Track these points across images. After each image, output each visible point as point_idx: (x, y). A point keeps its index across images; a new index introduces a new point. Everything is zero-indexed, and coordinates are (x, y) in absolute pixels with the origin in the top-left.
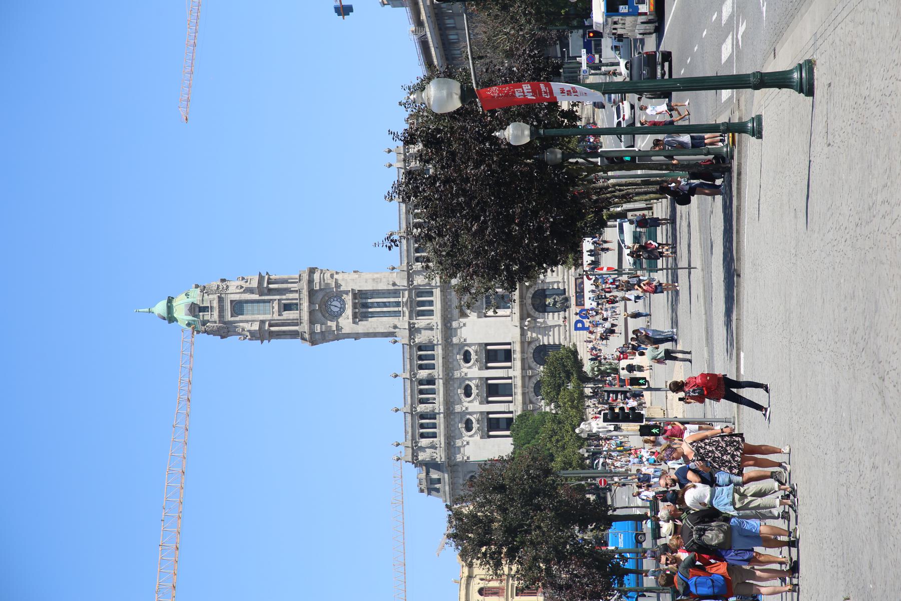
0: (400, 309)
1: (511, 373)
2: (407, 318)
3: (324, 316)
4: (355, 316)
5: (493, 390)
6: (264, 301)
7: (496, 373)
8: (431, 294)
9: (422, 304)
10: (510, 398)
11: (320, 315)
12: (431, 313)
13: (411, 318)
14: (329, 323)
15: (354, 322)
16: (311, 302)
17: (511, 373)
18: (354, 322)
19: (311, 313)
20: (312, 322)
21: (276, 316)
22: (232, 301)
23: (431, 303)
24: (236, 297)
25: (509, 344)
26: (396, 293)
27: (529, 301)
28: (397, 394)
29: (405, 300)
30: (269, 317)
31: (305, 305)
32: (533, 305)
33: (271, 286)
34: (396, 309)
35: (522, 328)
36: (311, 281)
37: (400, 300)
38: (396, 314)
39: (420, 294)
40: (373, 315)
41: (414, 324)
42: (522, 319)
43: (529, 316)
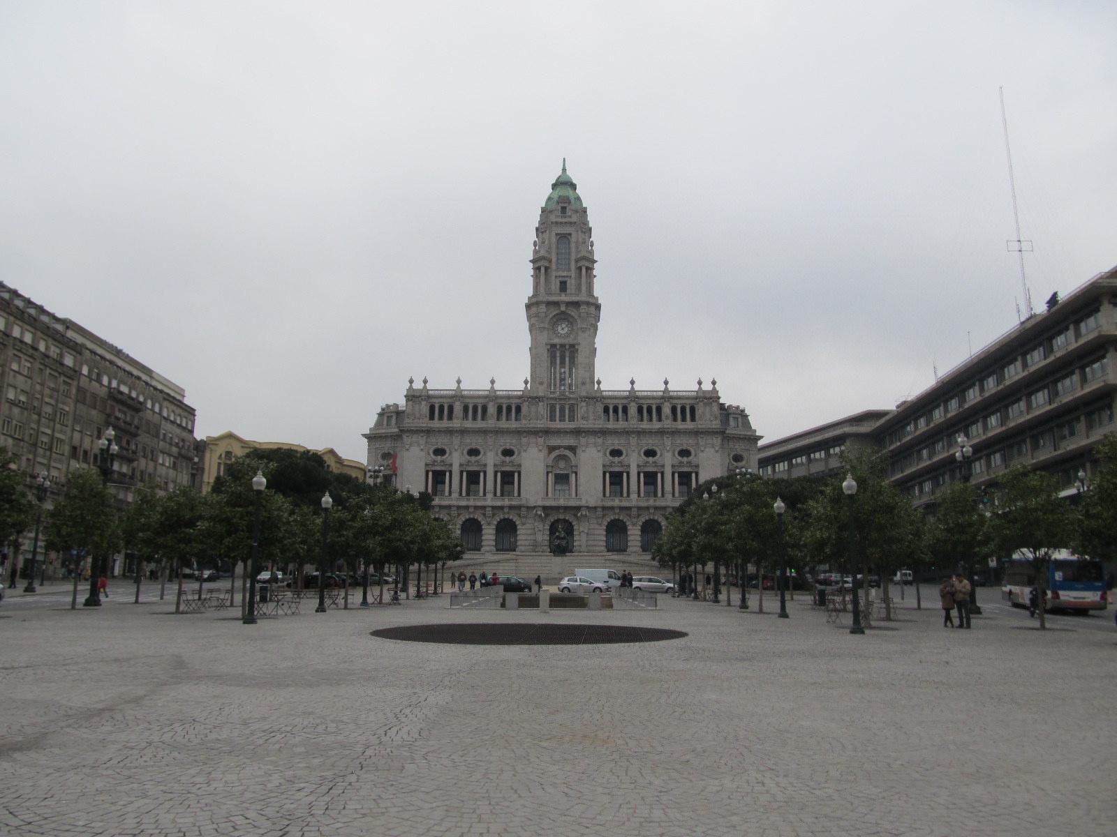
1: (490, 496)
3: (554, 316)
4: (553, 346)
5: (473, 478)
7: (490, 481)
8: (572, 419)
9: (562, 410)
10: (464, 493)
11: (555, 313)
12: (552, 419)
16: (569, 304)
17: (490, 496)
19: (557, 304)
21: (554, 274)
22: (570, 234)
23: (562, 419)
24: (573, 239)
25: (519, 495)
27: (562, 517)
28: (476, 383)
30: (554, 266)
31: (563, 298)
32: (557, 521)
33: (584, 270)
35: (535, 507)
36: (588, 304)
42: (545, 508)
43: (547, 515)
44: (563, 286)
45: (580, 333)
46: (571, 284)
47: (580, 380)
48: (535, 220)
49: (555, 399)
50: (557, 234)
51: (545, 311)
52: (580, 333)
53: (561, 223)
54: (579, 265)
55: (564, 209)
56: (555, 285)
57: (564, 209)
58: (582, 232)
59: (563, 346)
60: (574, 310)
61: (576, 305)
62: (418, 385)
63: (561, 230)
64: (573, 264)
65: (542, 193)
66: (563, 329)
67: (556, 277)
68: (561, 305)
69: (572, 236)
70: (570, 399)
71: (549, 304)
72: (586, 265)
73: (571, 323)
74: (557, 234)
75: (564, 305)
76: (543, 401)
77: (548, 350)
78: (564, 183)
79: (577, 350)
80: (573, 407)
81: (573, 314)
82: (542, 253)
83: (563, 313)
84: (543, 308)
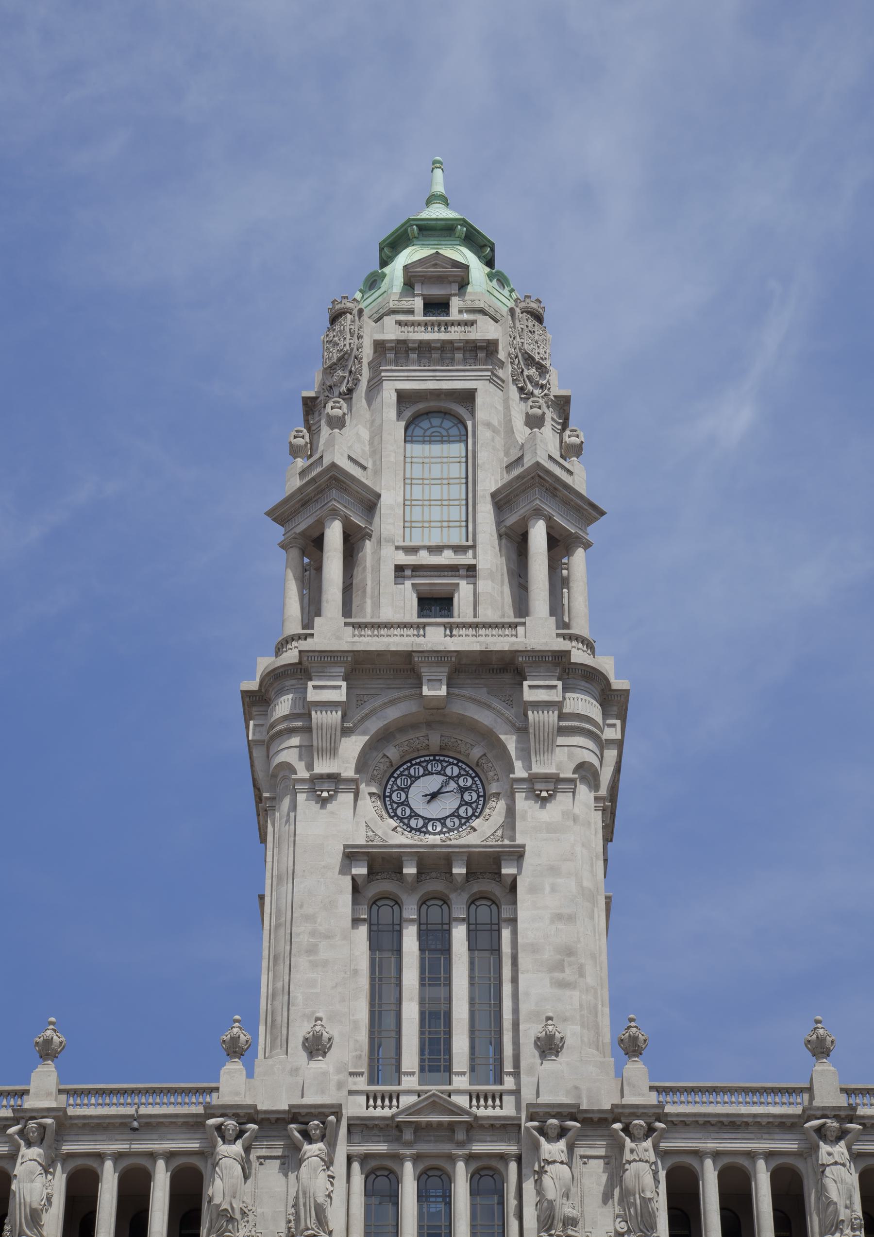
0: (410, 1082)
2: (357, 1107)
6: (470, 503)
11: (393, 714)
13: (361, 1128)
14: (352, 747)
15: (351, 856)
16: (466, 669)
18: (351, 856)
19: (405, 668)
20: (360, 668)
22: (468, 397)
26: (490, 1060)
29: (462, 1101)
33: (538, 534)
34: (410, 1058)
37: (461, 1082)
38: (382, 1059)
39: (487, 1178)
40: (384, 944)
41: (327, 1136)
44: (435, 604)
45: (522, 803)
47: (530, 1031)
49: (390, 1129)
50: (403, 398)
51: (340, 695)
52: (522, 803)
53: (424, 349)
54: (512, 519)
58: (521, 390)
59: (434, 864)
60: (496, 704)
61: (504, 671)
64: (486, 512)
67: (400, 569)
68: (426, 672)
69: (479, 400)
70: (476, 1127)
73: (476, 771)
74: (403, 398)
75: (443, 673)
76: (327, 1136)
77: (356, 889)
79: (513, 888)
80: (499, 1179)
81: (484, 718)
83: (435, 716)
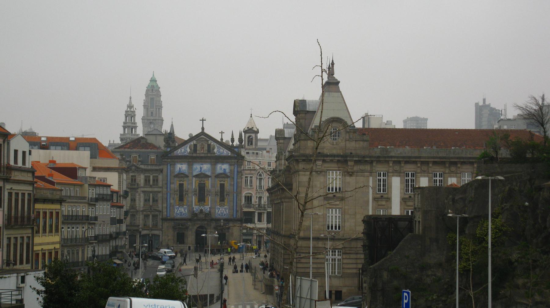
36: (159, 120)
46: (154, 113)
48: (144, 93)
55: (152, 90)
56: (150, 113)
57: (152, 90)
61: (155, 120)
62: (112, 142)
63: (151, 97)
65: (147, 83)
66: (152, 126)
71: (148, 120)
72: (160, 107)
78: (153, 80)
82: (146, 104)
84: (146, 121)
